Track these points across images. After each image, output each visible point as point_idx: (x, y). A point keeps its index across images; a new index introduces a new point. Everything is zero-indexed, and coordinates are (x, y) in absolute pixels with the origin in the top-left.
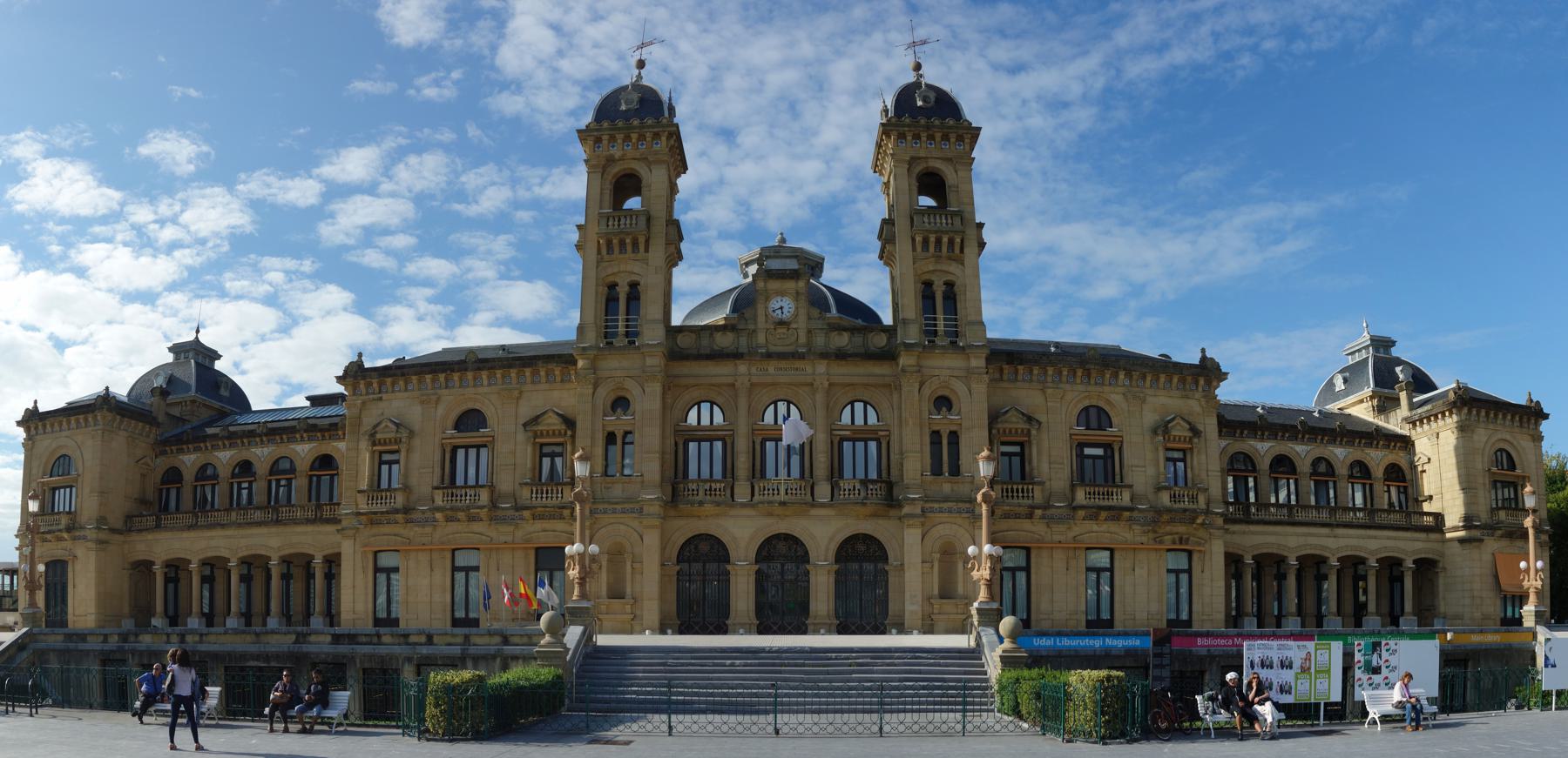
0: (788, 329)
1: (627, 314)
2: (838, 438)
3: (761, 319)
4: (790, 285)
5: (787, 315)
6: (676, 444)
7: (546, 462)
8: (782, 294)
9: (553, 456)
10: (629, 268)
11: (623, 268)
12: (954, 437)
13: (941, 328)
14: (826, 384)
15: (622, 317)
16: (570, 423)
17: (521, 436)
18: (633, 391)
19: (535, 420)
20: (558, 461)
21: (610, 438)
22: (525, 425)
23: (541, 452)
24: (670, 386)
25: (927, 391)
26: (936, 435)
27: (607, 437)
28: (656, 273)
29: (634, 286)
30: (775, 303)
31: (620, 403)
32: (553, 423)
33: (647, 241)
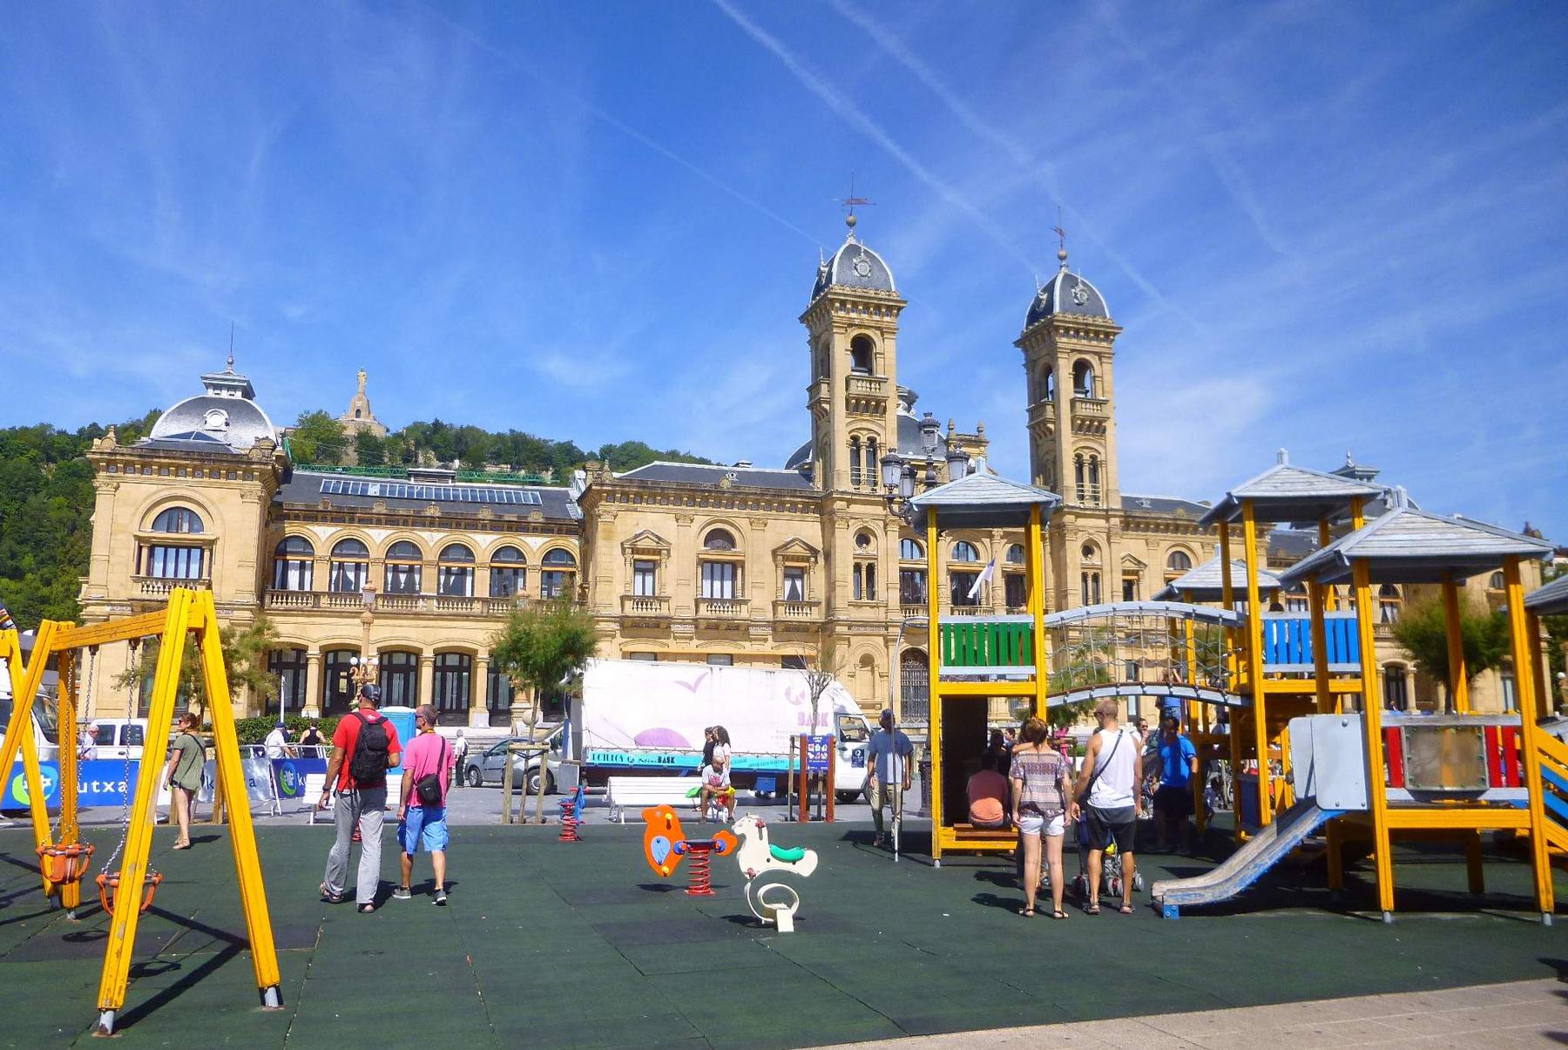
7: (788, 584)
10: (870, 426)
11: (865, 425)
12: (1096, 578)
19: (786, 546)
20: (798, 583)
21: (857, 568)
26: (1085, 577)
29: (872, 441)
32: (797, 550)
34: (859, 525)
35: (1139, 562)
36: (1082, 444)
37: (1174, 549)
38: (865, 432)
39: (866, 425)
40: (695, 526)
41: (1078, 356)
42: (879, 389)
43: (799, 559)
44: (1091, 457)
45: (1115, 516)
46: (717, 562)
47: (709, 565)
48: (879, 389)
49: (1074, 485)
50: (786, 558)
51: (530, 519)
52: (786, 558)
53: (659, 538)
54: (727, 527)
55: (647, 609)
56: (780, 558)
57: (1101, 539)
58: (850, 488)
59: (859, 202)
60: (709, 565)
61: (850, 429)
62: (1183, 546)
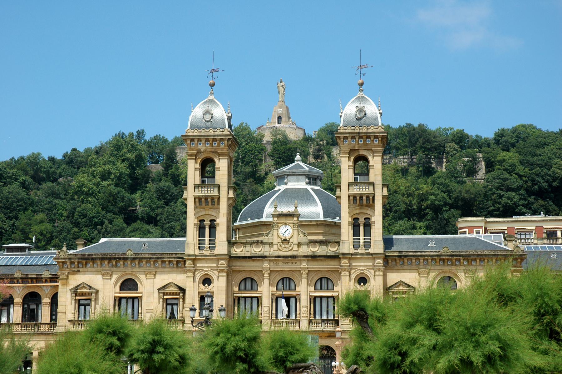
0: (289, 242)
1: (210, 238)
2: (313, 297)
3: (275, 237)
4: (289, 220)
5: (287, 236)
6: (234, 300)
8: (286, 224)
9: (172, 305)
10: (210, 213)
11: (207, 212)
13: (362, 244)
14: (307, 272)
15: (207, 238)
16: (183, 290)
17: (156, 294)
18: (214, 275)
19: (164, 287)
22: (159, 289)
23: (167, 303)
24: (230, 273)
25: (353, 277)
27: (200, 298)
28: (223, 217)
30: (283, 229)
31: (207, 281)
32: (173, 289)
33: (219, 199)
34: (203, 273)
35: (409, 286)
36: (358, 211)
37: (443, 275)
38: (207, 216)
39: (207, 213)
40: (115, 277)
41: (356, 154)
42: (213, 191)
43: (173, 294)
44: (365, 219)
45: (379, 258)
46: (131, 298)
47: (131, 300)
48: (213, 191)
49: (351, 239)
50: (164, 294)
51: (43, 276)
52: (164, 294)
53: (90, 287)
54: (129, 277)
55: (82, 327)
56: (162, 294)
57: (370, 273)
58: (197, 252)
59: (217, 70)
60: (125, 300)
61: (198, 216)
62: (450, 272)
